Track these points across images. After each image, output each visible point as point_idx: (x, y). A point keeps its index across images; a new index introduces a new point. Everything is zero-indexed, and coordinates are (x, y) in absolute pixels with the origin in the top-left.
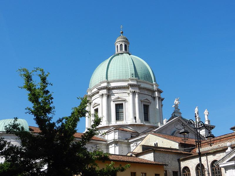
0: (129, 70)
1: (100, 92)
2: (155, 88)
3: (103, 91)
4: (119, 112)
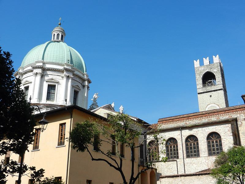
0: (66, 56)
1: (34, 70)
2: (85, 77)
3: (38, 70)
4: (50, 93)
